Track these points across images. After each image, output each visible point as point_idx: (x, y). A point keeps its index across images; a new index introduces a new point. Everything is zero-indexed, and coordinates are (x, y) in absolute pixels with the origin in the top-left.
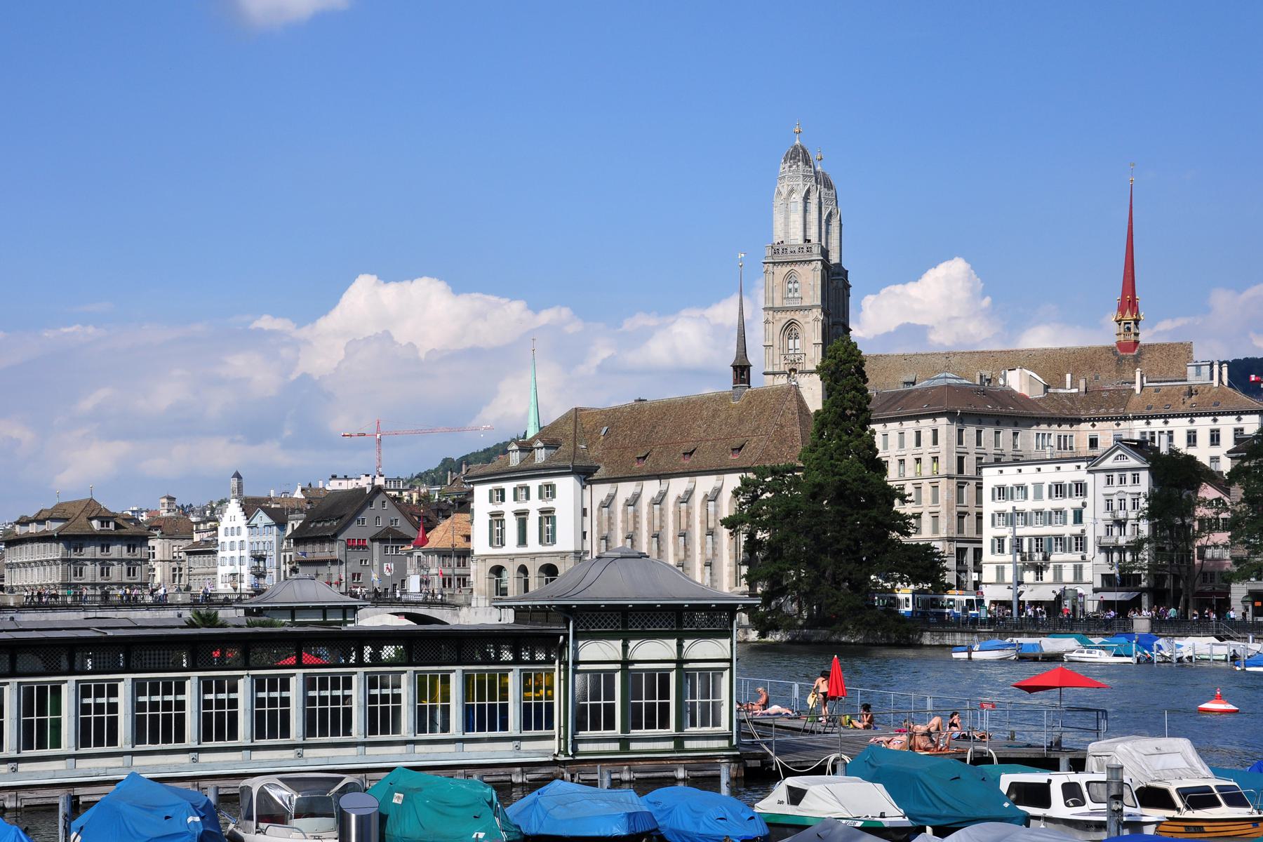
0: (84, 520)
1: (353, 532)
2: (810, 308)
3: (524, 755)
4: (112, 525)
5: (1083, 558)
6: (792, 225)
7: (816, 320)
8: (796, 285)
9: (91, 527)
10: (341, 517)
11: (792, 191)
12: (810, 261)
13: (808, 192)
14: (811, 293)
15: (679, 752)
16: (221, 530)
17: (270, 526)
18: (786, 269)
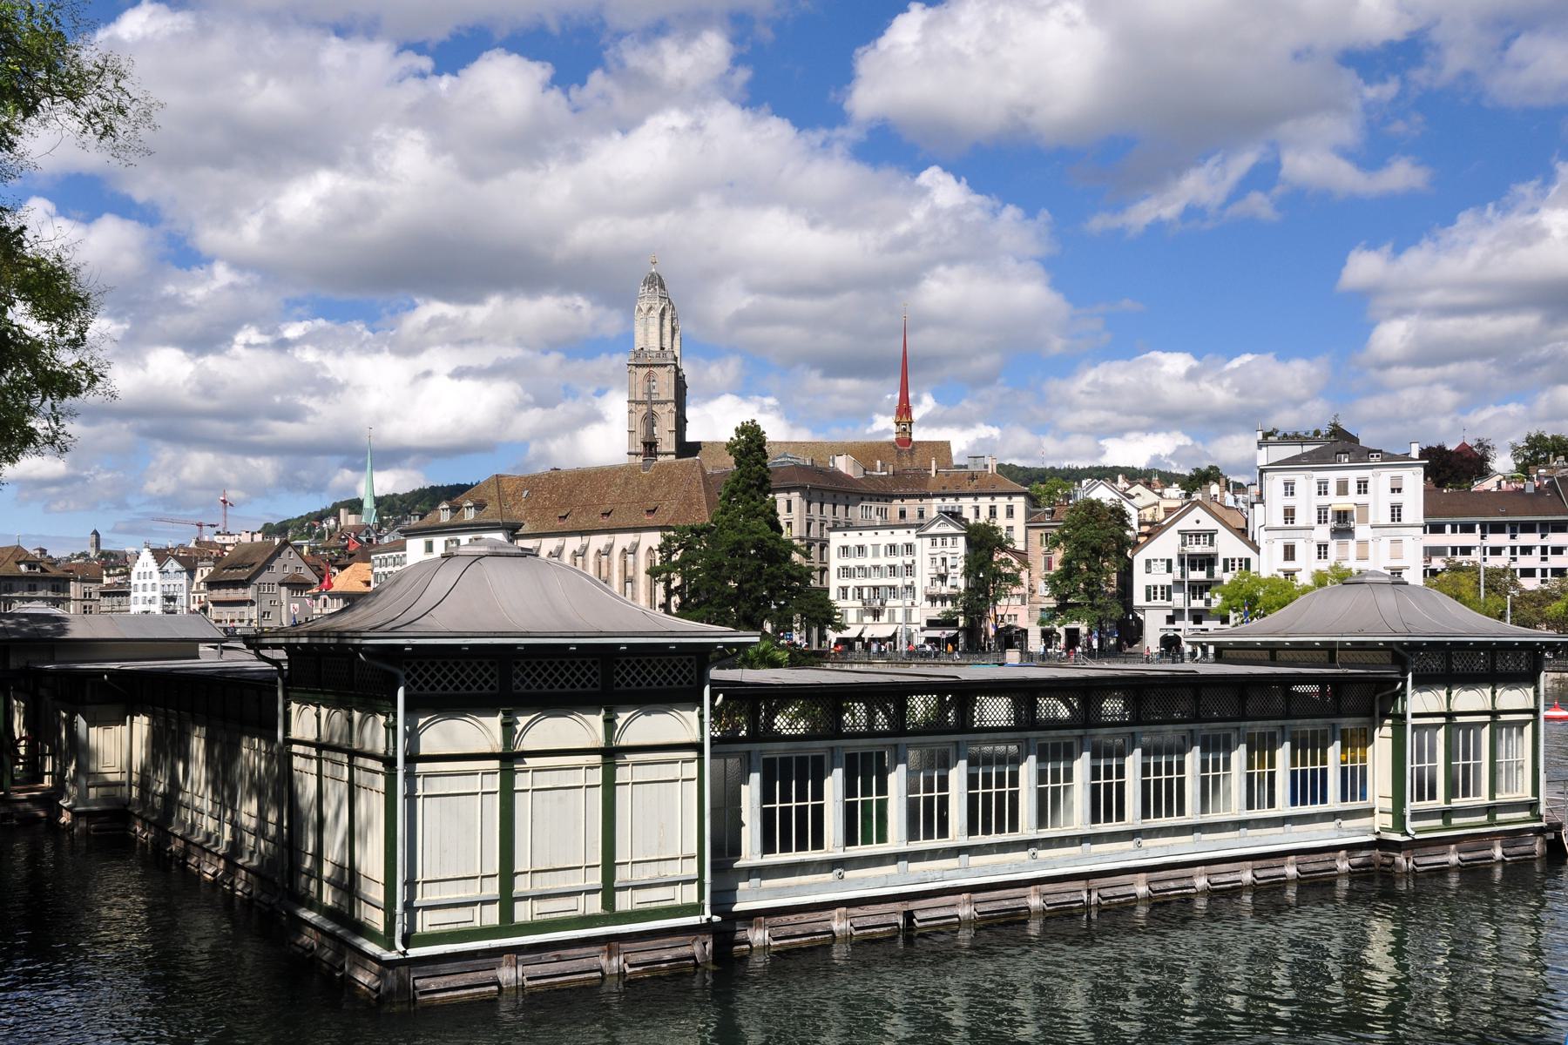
0: (13, 564)
1: (265, 577)
2: (665, 402)
3: (1346, 834)
4: (38, 570)
5: (913, 604)
6: (650, 335)
7: (670, 411)
8: (654, 384)
9: (19, 570)
10: (253, 565)
11: (650, 309)
12: (666, 365)
13: (664, 309)
14: (666, 390)
15: (1492, 825)
16: (134, 574)
17: (180, 572)
18: (646, 370)
